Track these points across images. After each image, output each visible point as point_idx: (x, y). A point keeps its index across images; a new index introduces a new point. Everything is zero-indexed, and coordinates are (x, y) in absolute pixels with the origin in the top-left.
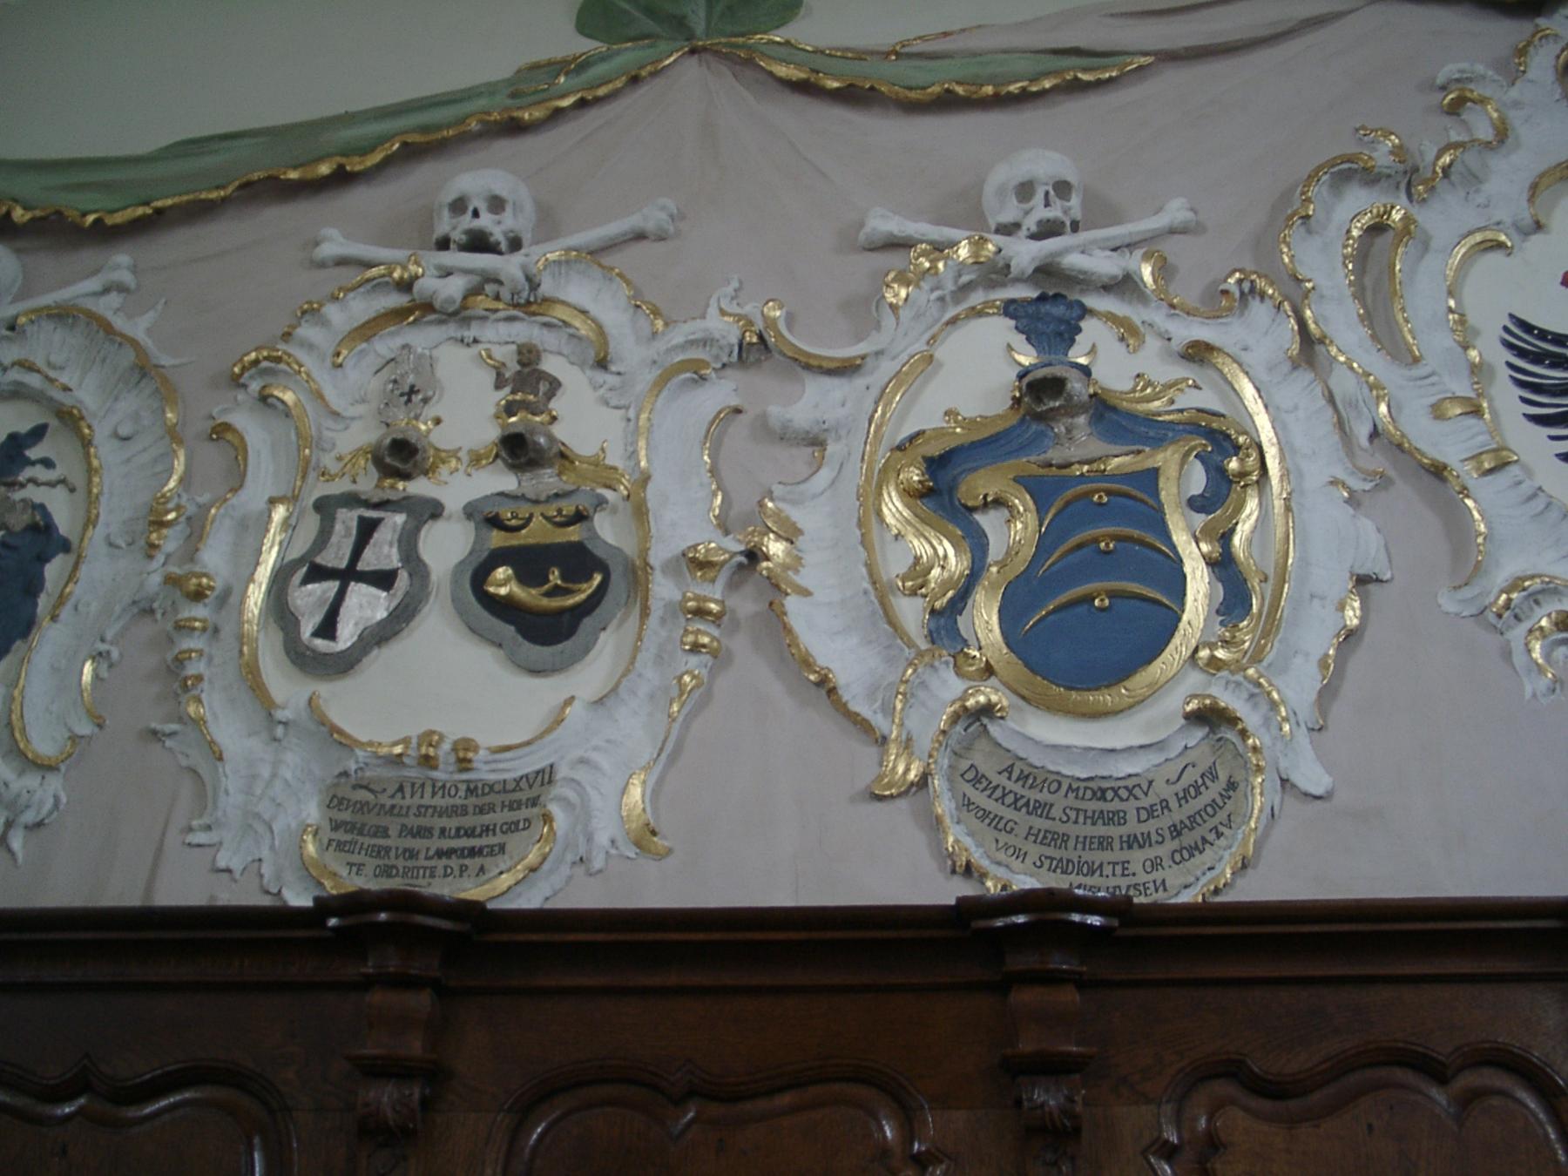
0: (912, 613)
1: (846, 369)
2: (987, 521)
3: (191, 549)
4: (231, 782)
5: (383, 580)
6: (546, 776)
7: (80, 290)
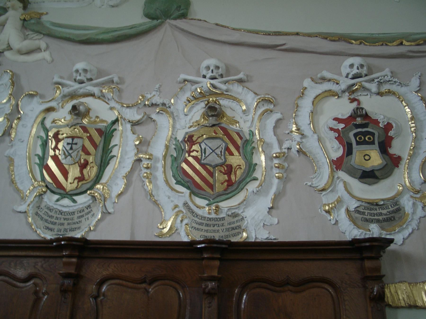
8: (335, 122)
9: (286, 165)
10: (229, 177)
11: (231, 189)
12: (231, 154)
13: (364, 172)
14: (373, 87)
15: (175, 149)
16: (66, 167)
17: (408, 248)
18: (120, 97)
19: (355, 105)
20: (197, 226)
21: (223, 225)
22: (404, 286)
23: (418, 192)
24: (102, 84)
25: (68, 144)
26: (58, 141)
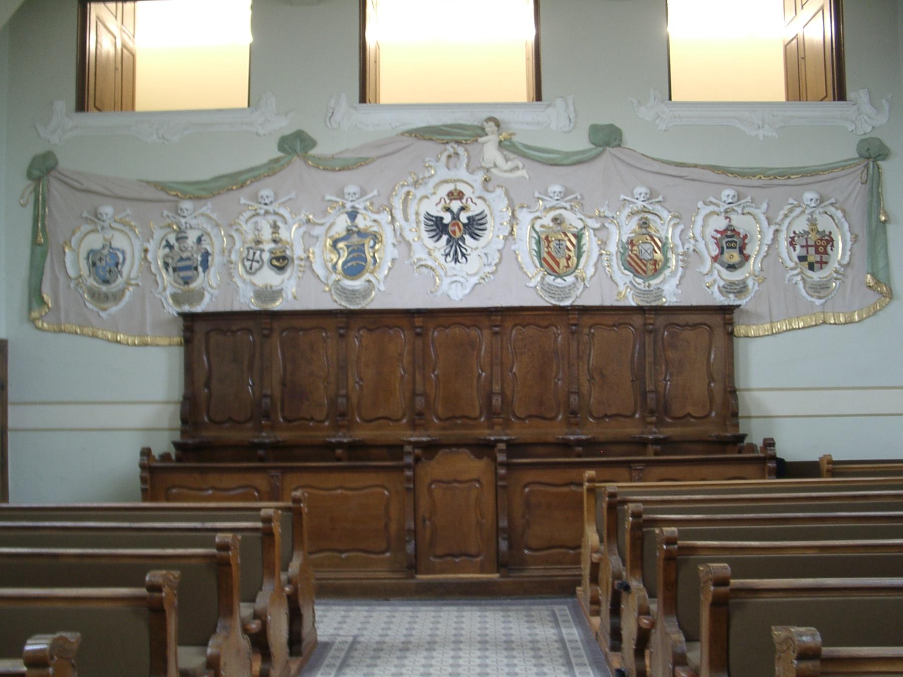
0: (330, 265)
1: (322, 225)
2: (341, 251)
3: (229, 256)
4: (241, 290)
5: (258, 262)
6: (282, 290)
7: (204, 209)
8: (715, 233)
9: (686, 259)
10: (655, 266)
11: (656, 273)
12: (656, 252)
13: (729, 265)
14: (739, 210)
15: (622, 247)
16: (558, 260)
17: (747, 307)
18: (583, 210)
19: (728, 220)
20: (638, 295)
21: (652, 294)
22: (743, 327)
23: (756, 276)
24: (570, 201)
25: (557, 244)
26: (549, 242)
